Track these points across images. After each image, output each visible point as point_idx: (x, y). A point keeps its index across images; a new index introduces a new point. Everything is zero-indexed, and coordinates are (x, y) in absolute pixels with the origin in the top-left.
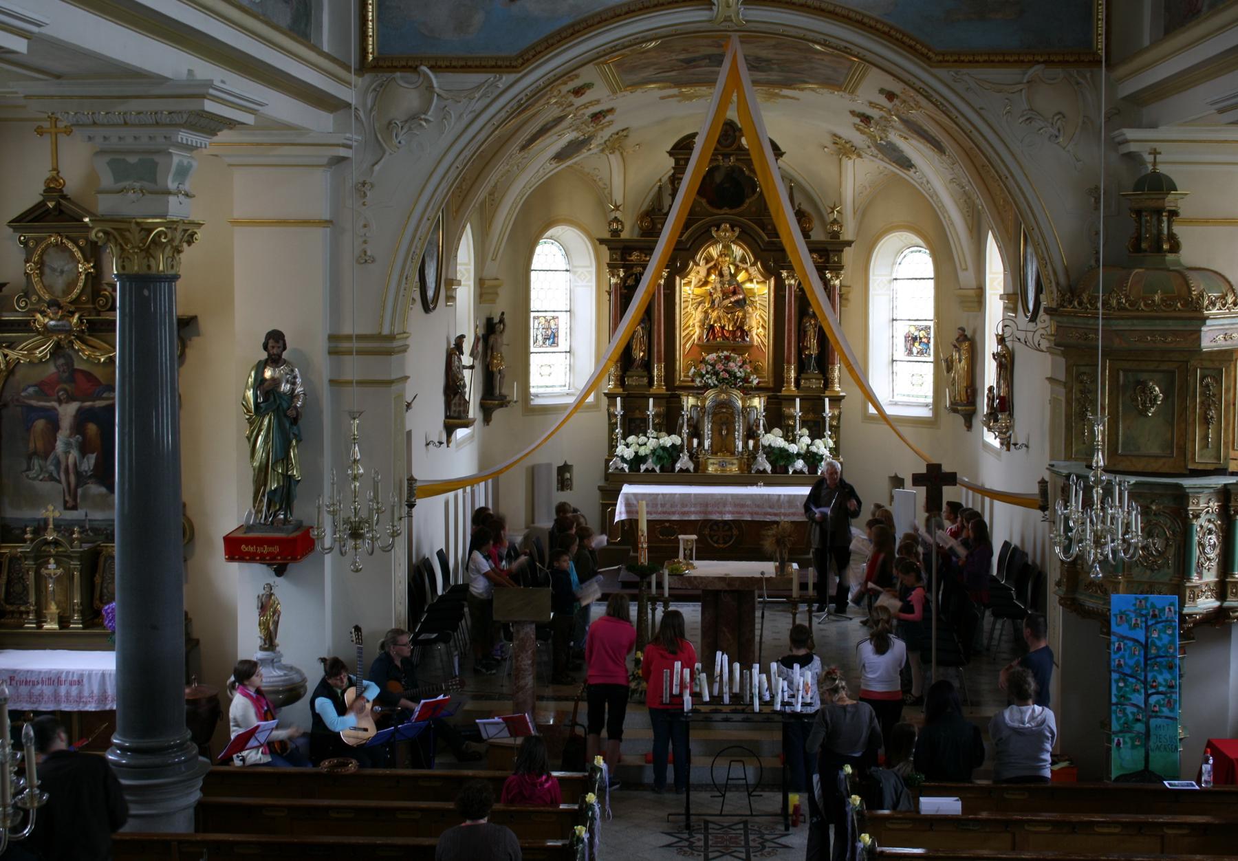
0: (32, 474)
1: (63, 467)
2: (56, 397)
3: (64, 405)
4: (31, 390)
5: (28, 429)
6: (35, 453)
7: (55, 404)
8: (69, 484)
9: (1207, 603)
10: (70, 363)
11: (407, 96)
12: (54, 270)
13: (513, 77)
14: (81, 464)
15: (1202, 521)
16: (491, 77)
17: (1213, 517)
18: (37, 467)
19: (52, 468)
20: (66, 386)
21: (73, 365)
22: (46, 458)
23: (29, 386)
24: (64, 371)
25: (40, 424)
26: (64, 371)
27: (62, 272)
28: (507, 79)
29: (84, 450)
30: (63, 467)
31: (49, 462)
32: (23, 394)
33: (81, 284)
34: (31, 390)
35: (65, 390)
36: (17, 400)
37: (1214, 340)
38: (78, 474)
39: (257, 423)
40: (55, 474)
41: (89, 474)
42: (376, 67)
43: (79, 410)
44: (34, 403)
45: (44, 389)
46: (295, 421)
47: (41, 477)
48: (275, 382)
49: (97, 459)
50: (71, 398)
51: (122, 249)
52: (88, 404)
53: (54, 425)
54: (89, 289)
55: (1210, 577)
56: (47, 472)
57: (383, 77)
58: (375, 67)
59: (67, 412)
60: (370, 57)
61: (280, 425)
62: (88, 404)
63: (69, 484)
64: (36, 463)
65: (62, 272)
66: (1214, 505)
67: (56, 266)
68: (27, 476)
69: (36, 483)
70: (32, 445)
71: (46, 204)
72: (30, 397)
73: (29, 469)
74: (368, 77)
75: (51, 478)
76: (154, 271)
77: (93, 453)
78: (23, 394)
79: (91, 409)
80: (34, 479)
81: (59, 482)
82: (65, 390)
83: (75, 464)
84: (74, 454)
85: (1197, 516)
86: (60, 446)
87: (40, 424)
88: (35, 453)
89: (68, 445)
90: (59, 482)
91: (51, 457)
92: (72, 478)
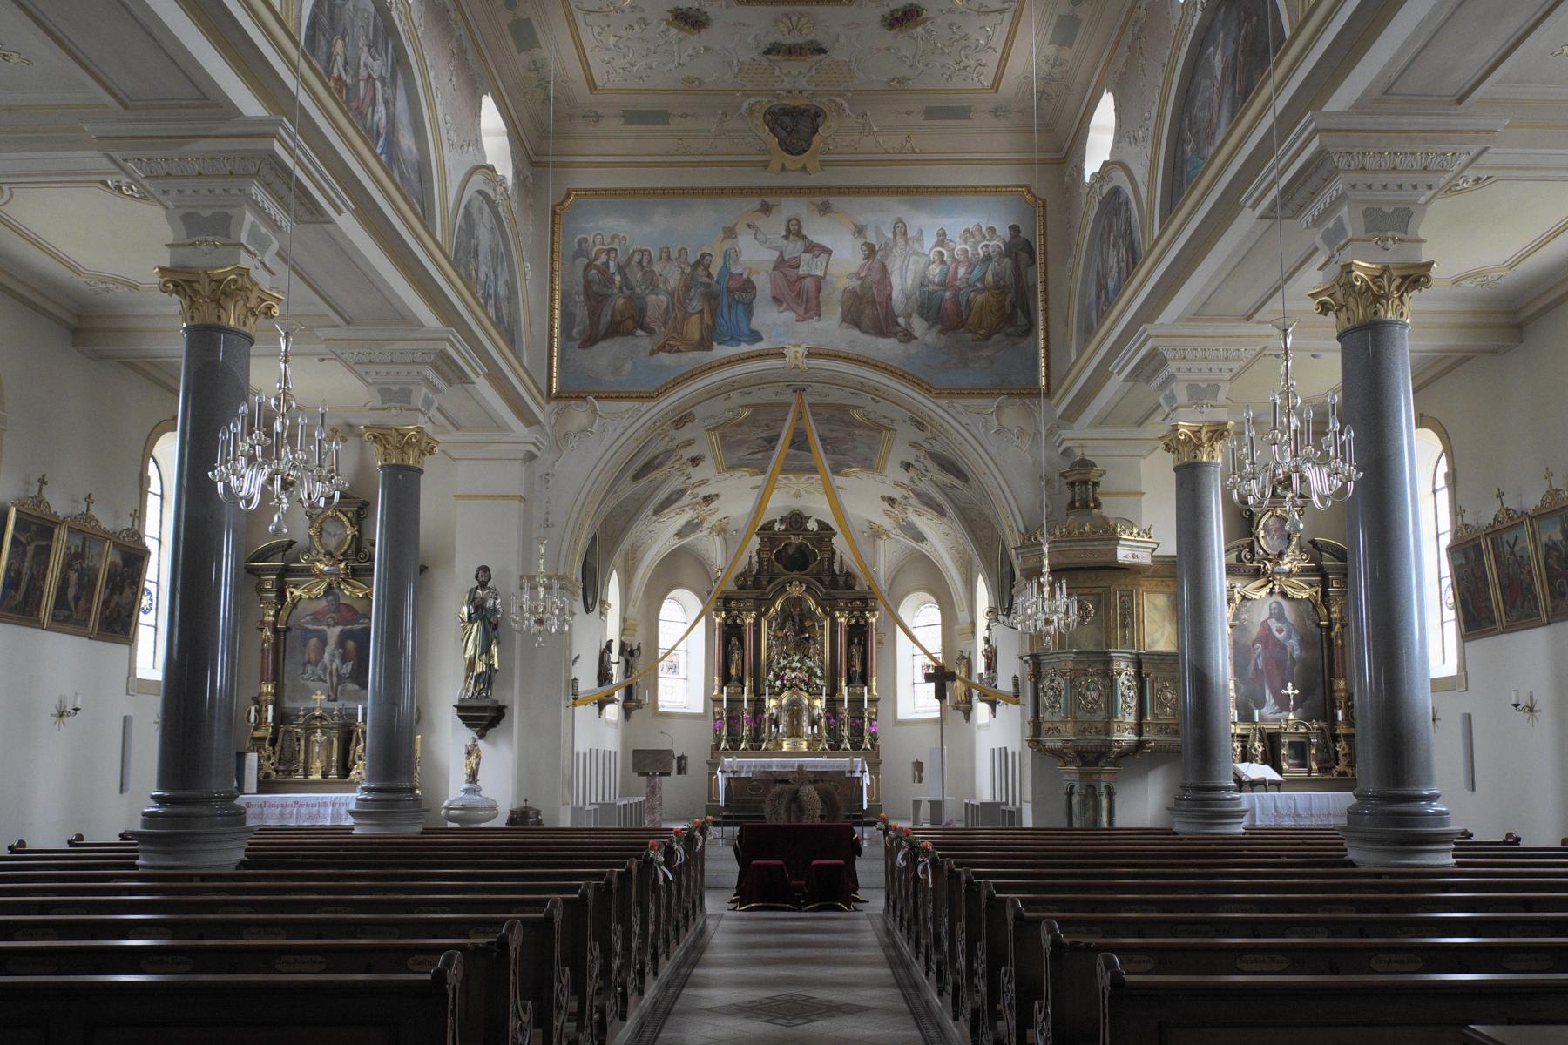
0: (306, 676)
1: (328, 671)
4: (308, 618)
5: (305, 646)
6: (309, 662)
7: (325, 628)
8: (332, 683)
9: (1129, 737)
11: (579, 415)
12: (330, 534)
13: (651, 404)
15: (1123, 678)
16: (636, 404)
17: (1131, 678)
18: (310, 672)
19: (320, 672)
25: (313, 642)
28: (646, 405)
29: (344, 659)
30: (328, 671)
33: (348, 543)
37: (1126, 557)
38: (339, 676)
39: (469, 628)
40: (322, 677)
42: (558, 397)
43: (342, 631)
44: (310, 627)
45: (317, 617)
46: (495, 627)
48: (484, 600)
50: (337, 624)
51: (385, 448)
54: (354, 546)
55: (1131, 719)
57: (562, 404)
58: (557, 398)
59: (334, 633)
60: (554, 391)
61: (485, 631)
63: (332, 683)
64: (309, 668)
65: (335, 535)
66: (1131, 670)
69: (309, 683)
72: (307, 623)
73: (304, 673)
74: (553, 404)
75: (320, 679)
76: (406, 463)
79: (351, 630)
81: (325, 681)
83: (337, 669)
84: (337, 662)
85: (1120, 674)
86: (327, 656)
88: (309, 662)
89: (333, 656)
90: (325, 681)
91: (320, 664)
92: (335, 679)
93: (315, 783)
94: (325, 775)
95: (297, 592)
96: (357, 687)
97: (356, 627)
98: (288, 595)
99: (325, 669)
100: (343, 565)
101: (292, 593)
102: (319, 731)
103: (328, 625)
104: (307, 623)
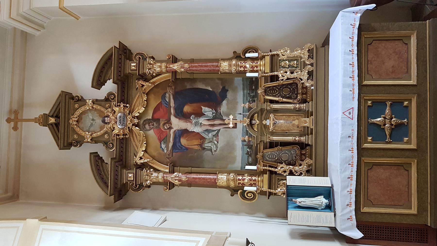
0: (214, 148)
2: (168, 130)
3: (173, 126)
4: (163, 146)
5: (187, 149)
6: (201, 145)
7: (172, 131)
8: (220, 124)
10: (148, 121)
12: (92, 125)
14: (208, 116)
18: (210, 145)
19: (210, 135)
20: (161, 124)
21: (150, 119)
22: (203, 138)
23: (161, 147)
24: (153, 125)
25: (184, 141)
26: (153, 125)
27: (93, 120)
29: (200, 114)
31: (207, 137)
32: (165, 151)
33: (99, 107)
34: (163, 146)
35: (164, 124)
36: (169, 155)
38: (214, 118)
40: (214, 133)
41: (214, 111)
43: (176, 117)
44: (171, 145)
45: (163, 138)
47: (216, 143)
49: (205, 106)
50: (169, 121)
52: (172, 111)
53: (184, 132)
54: (103, 103)
56: (213, 139)
62: (172, 111)
63: (220, 124)
65: (93, 120)
67: (90, 124)
68: (215, 151)
69: (219, 145)
70: (196, 147)
71: (51, 124)
72: (167, 147)
73: (211, 150)
75: (217, 135)
77: (202, 109)
78: (165, 151)
79: (175, 109)
80: (217, 147)
82: (164, 124)
83: (208, 120)
84: (202, 120)
86: (197, 130)
87: (184, 141)
88: (201, 145)
89: (196, 124)
91: (203, 135)
92: (217, 122)
93: (316, 123)
94: (308, 114)
95: (141, 154)
96: (225, 102)
97: (172, 104)
98: (142, 161)
99: (208, 131)
100: (116, 109)
101: (141, 158)
102: (264, 122)
103: (170, 128)
104: (167, 147)
